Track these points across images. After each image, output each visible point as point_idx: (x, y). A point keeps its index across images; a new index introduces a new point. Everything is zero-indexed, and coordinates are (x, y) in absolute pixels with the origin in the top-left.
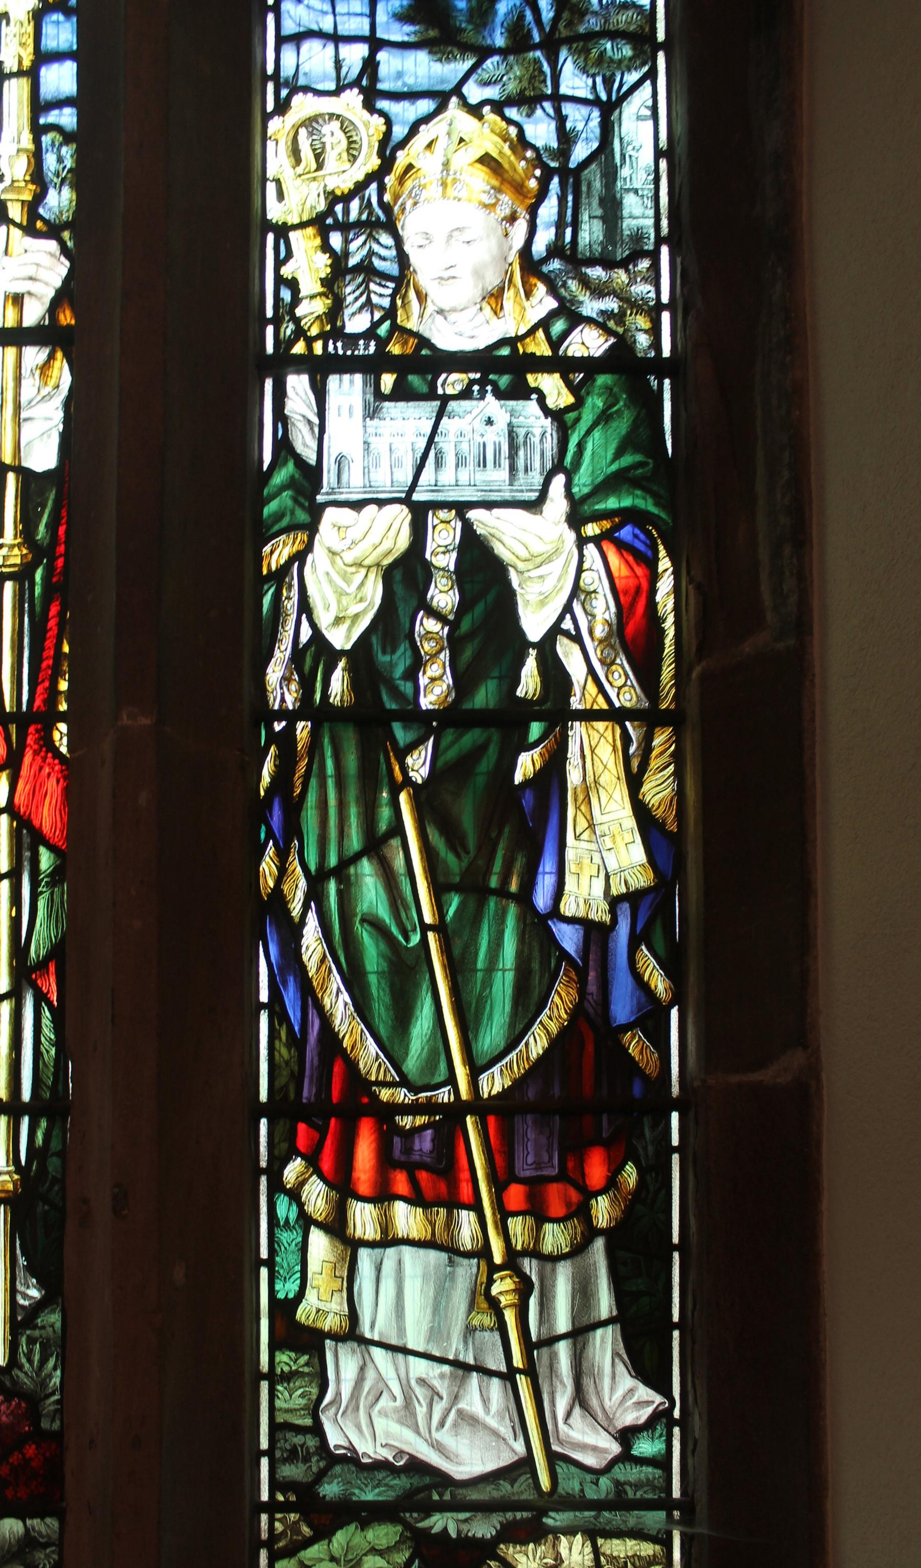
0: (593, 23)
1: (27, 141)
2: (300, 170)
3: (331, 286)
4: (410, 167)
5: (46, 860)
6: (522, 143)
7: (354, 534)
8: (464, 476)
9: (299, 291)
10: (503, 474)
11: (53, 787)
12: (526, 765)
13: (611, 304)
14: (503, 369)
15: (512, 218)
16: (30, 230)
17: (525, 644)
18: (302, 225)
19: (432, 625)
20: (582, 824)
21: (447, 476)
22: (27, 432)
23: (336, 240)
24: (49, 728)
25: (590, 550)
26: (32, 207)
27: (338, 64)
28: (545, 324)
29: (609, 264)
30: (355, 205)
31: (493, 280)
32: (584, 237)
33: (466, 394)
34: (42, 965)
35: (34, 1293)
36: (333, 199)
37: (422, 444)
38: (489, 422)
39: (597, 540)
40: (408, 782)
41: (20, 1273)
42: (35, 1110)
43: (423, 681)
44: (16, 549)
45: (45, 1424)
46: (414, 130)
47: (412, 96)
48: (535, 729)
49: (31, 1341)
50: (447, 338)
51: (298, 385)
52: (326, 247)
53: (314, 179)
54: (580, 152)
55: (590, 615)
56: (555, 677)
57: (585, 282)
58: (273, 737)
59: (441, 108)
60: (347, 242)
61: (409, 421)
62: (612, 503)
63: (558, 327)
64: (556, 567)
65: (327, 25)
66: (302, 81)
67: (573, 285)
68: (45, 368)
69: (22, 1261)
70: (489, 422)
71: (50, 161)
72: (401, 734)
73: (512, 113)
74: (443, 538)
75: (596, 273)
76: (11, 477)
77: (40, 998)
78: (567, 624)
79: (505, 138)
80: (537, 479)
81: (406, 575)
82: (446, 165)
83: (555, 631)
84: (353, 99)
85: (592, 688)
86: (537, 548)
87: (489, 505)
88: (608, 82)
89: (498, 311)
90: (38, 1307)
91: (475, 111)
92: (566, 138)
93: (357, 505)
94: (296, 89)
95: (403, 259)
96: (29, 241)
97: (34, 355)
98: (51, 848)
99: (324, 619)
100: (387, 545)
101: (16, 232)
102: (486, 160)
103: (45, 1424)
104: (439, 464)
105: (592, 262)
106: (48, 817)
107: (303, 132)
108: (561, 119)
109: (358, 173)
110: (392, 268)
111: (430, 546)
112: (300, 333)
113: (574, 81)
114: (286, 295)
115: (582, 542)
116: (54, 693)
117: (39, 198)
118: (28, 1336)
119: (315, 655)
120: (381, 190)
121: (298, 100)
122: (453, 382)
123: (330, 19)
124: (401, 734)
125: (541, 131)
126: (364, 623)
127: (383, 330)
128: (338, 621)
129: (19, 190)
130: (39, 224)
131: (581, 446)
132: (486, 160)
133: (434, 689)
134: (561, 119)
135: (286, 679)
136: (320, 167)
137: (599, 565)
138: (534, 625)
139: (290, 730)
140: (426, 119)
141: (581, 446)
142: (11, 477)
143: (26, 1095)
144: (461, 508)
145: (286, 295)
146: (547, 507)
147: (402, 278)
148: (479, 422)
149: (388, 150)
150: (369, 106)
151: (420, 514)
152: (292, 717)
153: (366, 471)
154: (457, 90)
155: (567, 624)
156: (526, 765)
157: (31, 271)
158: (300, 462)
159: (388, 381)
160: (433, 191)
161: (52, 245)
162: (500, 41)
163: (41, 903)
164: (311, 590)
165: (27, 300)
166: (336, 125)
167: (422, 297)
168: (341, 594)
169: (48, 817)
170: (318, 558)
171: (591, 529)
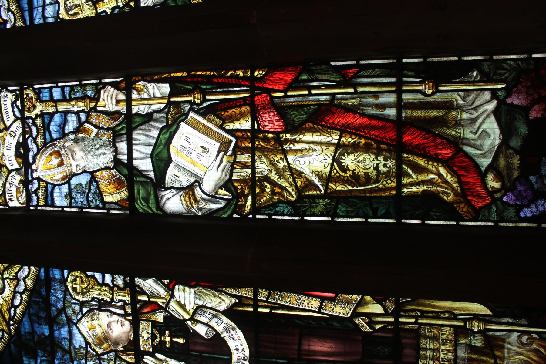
1: (73, 103)
2: (80, 12)
5: (305, 77)
9: (115, 6)
11: (277, 76)
16: (98, 100)
18: (96, 9)
22: (158, 95)
24: (256, 78)
26: (92, 99)
34: (343, 76)
35: (475, 74)
41: (467, 79)
42: (399, 76)
44: (196, 96)
45: (532, 67)
49: (495, 74)
53: (83, 7)
65: (40, 9)
66: (56, 15)
68: (138, 91)
69: (461, 79)
71: (79, 95)
76: (172, 99)
77: (356, 76)
90: (480, 72)
94: (58, 17)
96: (101, 100)
97: (135, 95)
98: (299, 75)
101: (99, 104)
103: (532, 67)
106: (288, 77)
107: (70, 13)
116: (245, 78)
117: (89, 97)
118: (494, 75)
121: (61, 16)
123: (39, 8)
129: (87, 104)
130: (96, 97)
136: (79, 5)
142: (172, 99)
143: (394, 80)
157: (109, 98)
161: (102, 92)
163: (320, 77)
165: (118, 99)
169: (288, 77)
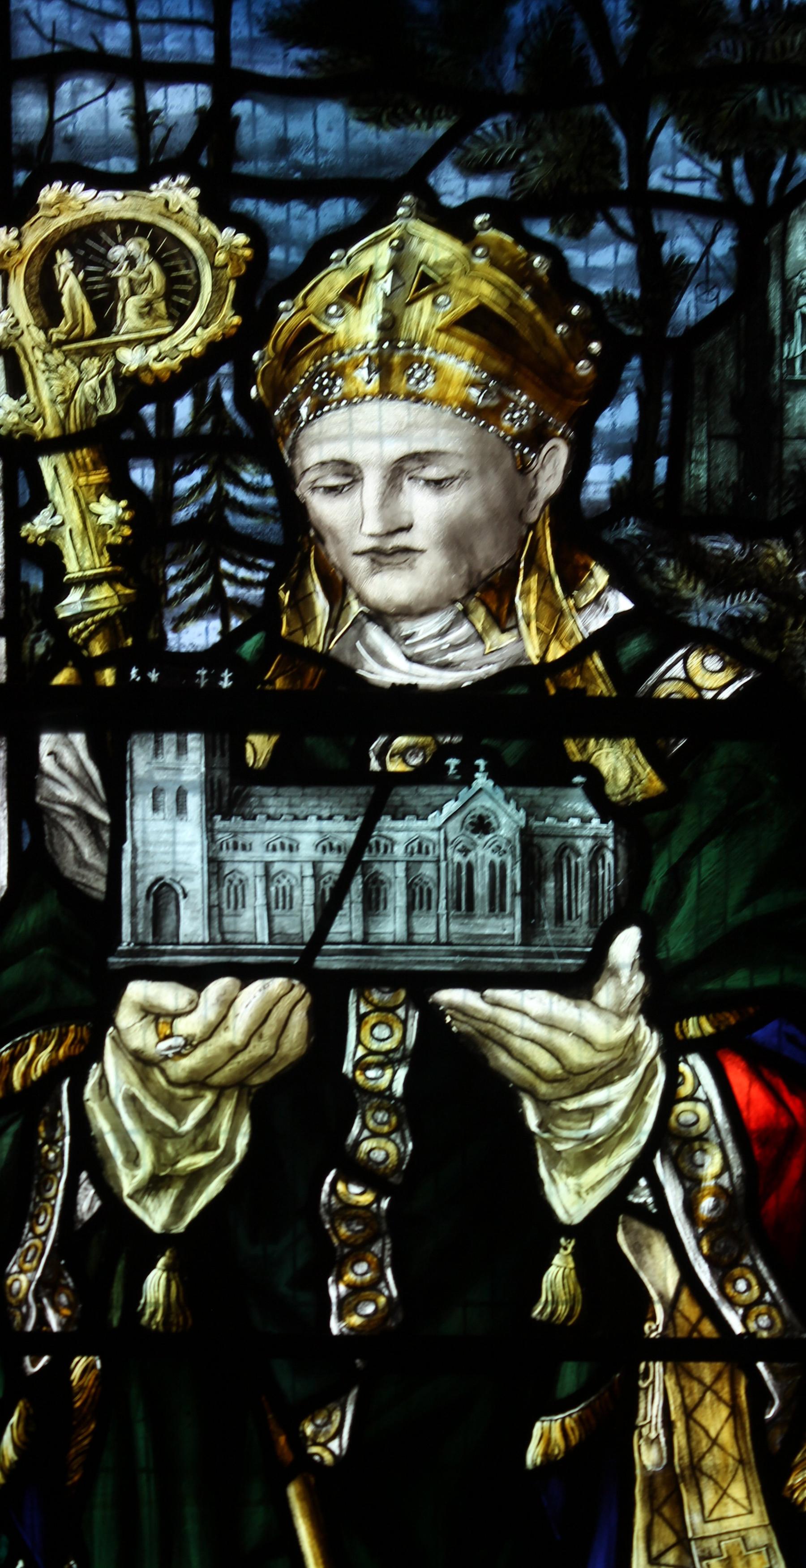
0: (727, 50)
2: (57, 334)
3: (135, 559)
4: (309, 331)
6: (561, 286)
7: (186, 1026)
8: (425, 928)
9: (63, 569)
10: (510, 926)
12: (546, 1437)
13: (748, 604)
14: (513, 727)
15: (536, 437)
17: (547, 1230)
19: (357, 1194)
20: (665, 1536)
21: (391, 926)
23: (143, 476)
25: (696, 1069)
27: (142, 118)
28: (604, 641)
29: (750, 530)
30: (184, 410)
31: (489, 554)
32: (699, 473)
33: (430, 774)
36: (133, 387)
37: (334, 865)
38: (482, 825)
39: (706, 1048)
40: (305, 1467)
43: (335, 1291)
46: (317, 258)
47: (313, 188)
48: (570, 1376)
50: (387, 664)
51: (63, 754)
52: (119, 487)
53: (92, 352)
54: (690, 307)
55: (691, 1183)
56: (610, 1282)
57: (699, 566)
58: (22, 1387)
59: (377, 216)
60: (166, 479)
61: (303, 837)
62: (738, 980)
63: (635, 648)
64: (621, 1092)
65: (117, 37)
66: (60, 154)
67: (668, 569)
70: (482, 825)
72: (288, 1381)
73: (542, 229)
74: (375, 1044)
75: (722, 545)
78: (643, 1196)
79: (521, 274)
80: (581, 933)
81: (297, 1103)
82: (389, 328)
83: (615, 1207)
84: (177, 194)
85: (689, 1308)
86: (578, 1055)
87: (478, 981)
88: (758, 174)
89: (503, 618)
91: (455, 222)
92: (661, 277)
93: (195, 978)
95: (294, 515)
99: (128, 1181)
100: (259, 1048)
102: (476, 322)
104: (373, 903)
105: (716, 525)
107: (64, 261)
108: (648, 243)
109: (190, 339)
110: (273, 531)
111: (352, 1051)
112: (66, 650)
113: (678, 168)
114: (36, 581)
115: (673, 1051)
119: (109, 1245)
120: (244, 377)
122: (399, 753)
123: (123, 30)
124: (288, 1381)
125: (604, 261)
126: (215, 1187)
127: (249, 647)
128: (154, 1185)
131: (677, 877)
132: (476, 322)
133: (356, 1299)
134: (648, 243)
135: (47, 1287)
136: (106, 322)
137: (709, 1087)
138: (571, 1197)
139: (59, 1369)
140: (346, 236)
141: (677, 877)
144: (419, 986)
145: (36, 581)
146: (605, 994)
147: (295, 543)
148: (458, 830)
149: (260, 290)
150: (215, 208)
151: (328, 1001)
152: (63, 1347)
153: (214, 914)
154: (417, 181)
155: (643, 1196)
156: (546, 1437)
158: (71, 892)
159: (259, 747)
160: (362, 378)
162: (510, 76)
164: (101, 1123)
166: (135, 246)
167: (338, 588)
168: (159, 1135)
170: (114, 1068)
171: (695, 1027)
